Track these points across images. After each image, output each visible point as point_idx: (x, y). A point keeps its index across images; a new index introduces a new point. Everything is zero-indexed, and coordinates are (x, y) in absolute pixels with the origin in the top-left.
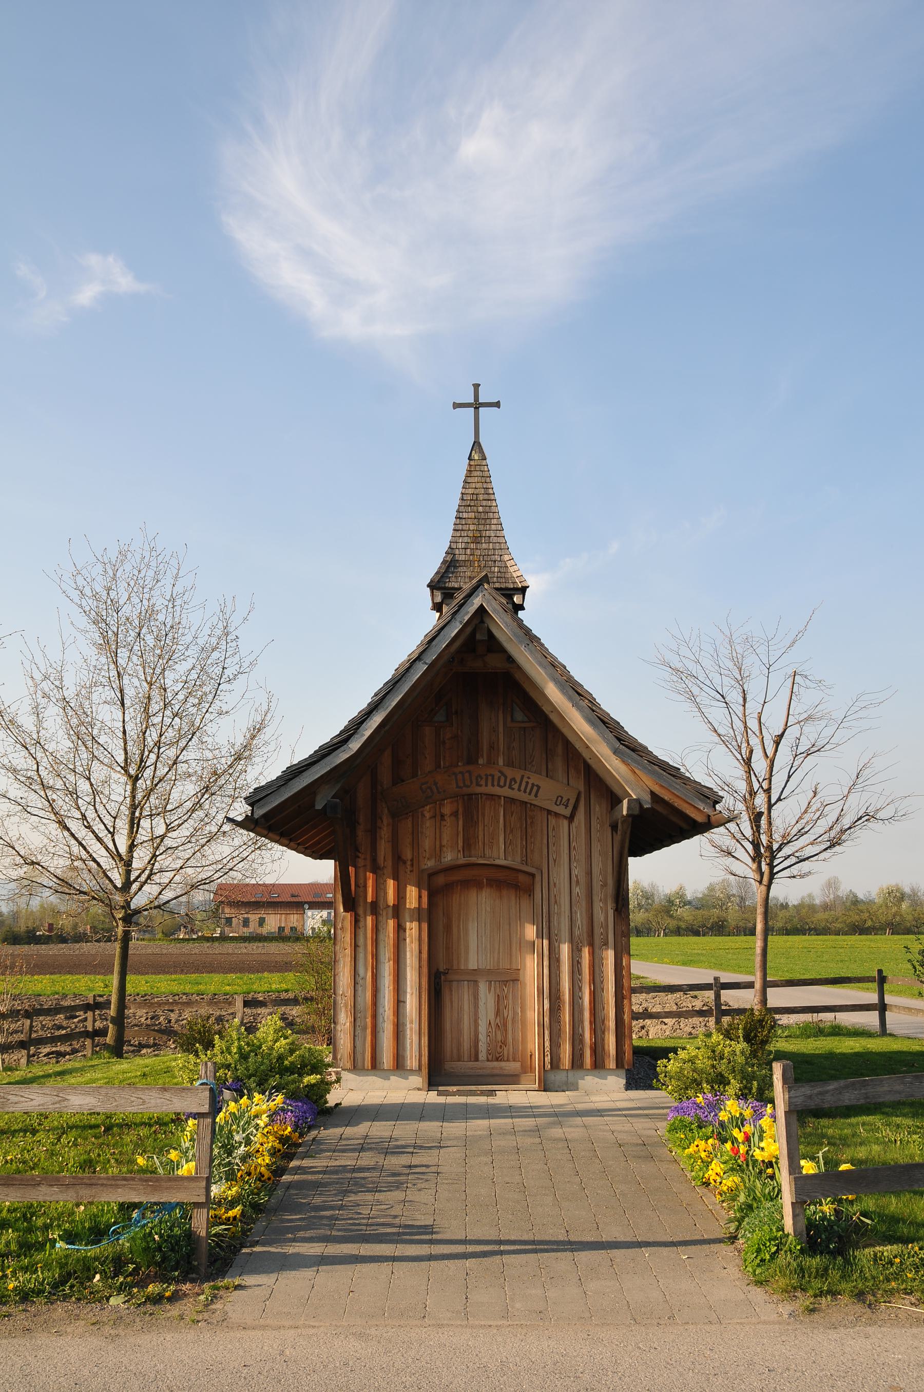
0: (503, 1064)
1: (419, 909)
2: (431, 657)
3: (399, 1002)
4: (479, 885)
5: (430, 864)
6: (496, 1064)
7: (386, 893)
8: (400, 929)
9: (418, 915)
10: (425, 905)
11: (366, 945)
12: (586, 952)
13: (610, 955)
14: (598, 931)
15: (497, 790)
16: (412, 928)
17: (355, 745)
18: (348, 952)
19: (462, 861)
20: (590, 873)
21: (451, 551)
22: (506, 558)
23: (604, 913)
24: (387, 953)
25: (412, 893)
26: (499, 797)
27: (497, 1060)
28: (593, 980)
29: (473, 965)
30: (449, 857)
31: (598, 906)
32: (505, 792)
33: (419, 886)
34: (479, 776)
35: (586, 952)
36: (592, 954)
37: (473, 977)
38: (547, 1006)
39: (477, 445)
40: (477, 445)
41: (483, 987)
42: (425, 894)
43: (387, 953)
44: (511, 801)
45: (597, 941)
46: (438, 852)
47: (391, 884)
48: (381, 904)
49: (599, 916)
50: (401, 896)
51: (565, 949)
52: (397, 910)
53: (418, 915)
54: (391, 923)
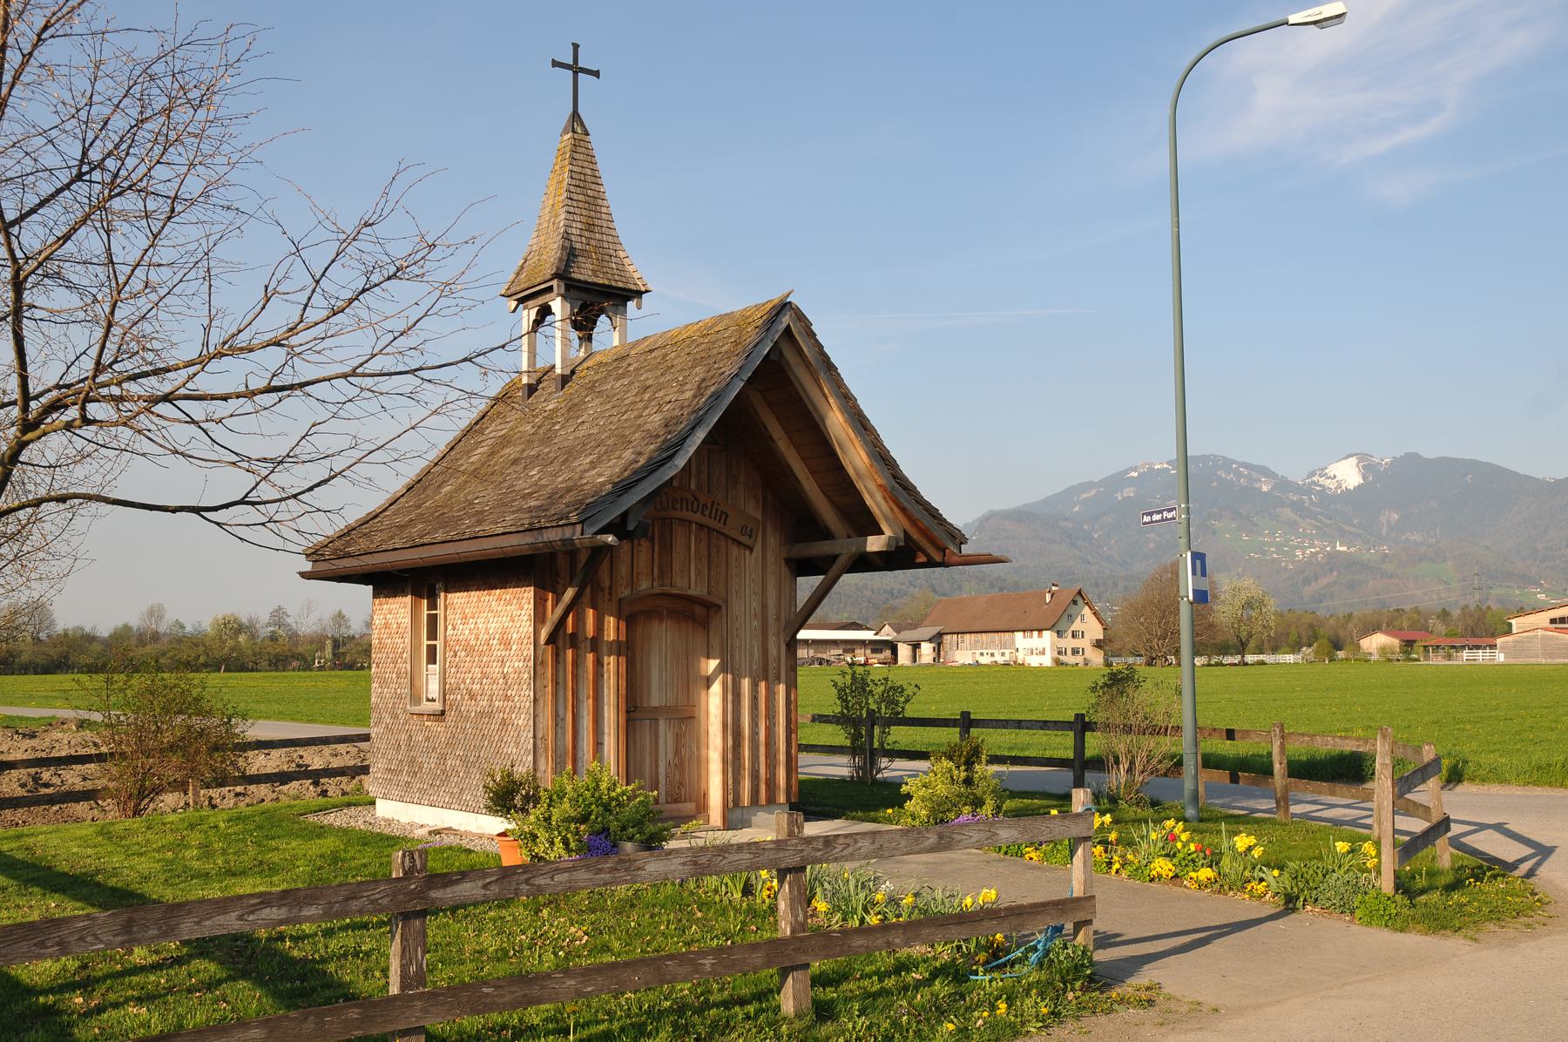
1: (618, 642)
3: (598, 745)
5: (625, 592)
7: (584, 624)
8: (599, 663)
10: (623, 638)
11: (565, 681)
12: (763, 685)
13: (782, 688)
14: (772, 664)
15: (690, 516)
16: (610, 662)
17: (681, 461)
18: (549, 689)
19: (657, 590)
20: (764, 606)
21: (566, 236)
22: (622, 254)
23: (775, 647)
24: (587, 690)
25: (611, 622)
26: (690, 522)
27: (676, 801)
28: (767, 717)
29: (655, 702)
30: (644, 585)
31: (772, 640)
32: (698, 517)
33: (619, 618)
35: (763, 685)
36: (767, 689)
37: (654, 714)
38: (730, 743)
39: (575, 116)
40: (575, 116)
41: (662, 724)
42: (623, 625)
43: (587, 690)
44: (701, 526)
46: (632, 582)
47: (590, 613)
48: (581, 637)
49: (773, 651)
50: (599, 627)
51: (746, 683)
52: (596, 644)
53: (619, 648)
54: (590, 657)
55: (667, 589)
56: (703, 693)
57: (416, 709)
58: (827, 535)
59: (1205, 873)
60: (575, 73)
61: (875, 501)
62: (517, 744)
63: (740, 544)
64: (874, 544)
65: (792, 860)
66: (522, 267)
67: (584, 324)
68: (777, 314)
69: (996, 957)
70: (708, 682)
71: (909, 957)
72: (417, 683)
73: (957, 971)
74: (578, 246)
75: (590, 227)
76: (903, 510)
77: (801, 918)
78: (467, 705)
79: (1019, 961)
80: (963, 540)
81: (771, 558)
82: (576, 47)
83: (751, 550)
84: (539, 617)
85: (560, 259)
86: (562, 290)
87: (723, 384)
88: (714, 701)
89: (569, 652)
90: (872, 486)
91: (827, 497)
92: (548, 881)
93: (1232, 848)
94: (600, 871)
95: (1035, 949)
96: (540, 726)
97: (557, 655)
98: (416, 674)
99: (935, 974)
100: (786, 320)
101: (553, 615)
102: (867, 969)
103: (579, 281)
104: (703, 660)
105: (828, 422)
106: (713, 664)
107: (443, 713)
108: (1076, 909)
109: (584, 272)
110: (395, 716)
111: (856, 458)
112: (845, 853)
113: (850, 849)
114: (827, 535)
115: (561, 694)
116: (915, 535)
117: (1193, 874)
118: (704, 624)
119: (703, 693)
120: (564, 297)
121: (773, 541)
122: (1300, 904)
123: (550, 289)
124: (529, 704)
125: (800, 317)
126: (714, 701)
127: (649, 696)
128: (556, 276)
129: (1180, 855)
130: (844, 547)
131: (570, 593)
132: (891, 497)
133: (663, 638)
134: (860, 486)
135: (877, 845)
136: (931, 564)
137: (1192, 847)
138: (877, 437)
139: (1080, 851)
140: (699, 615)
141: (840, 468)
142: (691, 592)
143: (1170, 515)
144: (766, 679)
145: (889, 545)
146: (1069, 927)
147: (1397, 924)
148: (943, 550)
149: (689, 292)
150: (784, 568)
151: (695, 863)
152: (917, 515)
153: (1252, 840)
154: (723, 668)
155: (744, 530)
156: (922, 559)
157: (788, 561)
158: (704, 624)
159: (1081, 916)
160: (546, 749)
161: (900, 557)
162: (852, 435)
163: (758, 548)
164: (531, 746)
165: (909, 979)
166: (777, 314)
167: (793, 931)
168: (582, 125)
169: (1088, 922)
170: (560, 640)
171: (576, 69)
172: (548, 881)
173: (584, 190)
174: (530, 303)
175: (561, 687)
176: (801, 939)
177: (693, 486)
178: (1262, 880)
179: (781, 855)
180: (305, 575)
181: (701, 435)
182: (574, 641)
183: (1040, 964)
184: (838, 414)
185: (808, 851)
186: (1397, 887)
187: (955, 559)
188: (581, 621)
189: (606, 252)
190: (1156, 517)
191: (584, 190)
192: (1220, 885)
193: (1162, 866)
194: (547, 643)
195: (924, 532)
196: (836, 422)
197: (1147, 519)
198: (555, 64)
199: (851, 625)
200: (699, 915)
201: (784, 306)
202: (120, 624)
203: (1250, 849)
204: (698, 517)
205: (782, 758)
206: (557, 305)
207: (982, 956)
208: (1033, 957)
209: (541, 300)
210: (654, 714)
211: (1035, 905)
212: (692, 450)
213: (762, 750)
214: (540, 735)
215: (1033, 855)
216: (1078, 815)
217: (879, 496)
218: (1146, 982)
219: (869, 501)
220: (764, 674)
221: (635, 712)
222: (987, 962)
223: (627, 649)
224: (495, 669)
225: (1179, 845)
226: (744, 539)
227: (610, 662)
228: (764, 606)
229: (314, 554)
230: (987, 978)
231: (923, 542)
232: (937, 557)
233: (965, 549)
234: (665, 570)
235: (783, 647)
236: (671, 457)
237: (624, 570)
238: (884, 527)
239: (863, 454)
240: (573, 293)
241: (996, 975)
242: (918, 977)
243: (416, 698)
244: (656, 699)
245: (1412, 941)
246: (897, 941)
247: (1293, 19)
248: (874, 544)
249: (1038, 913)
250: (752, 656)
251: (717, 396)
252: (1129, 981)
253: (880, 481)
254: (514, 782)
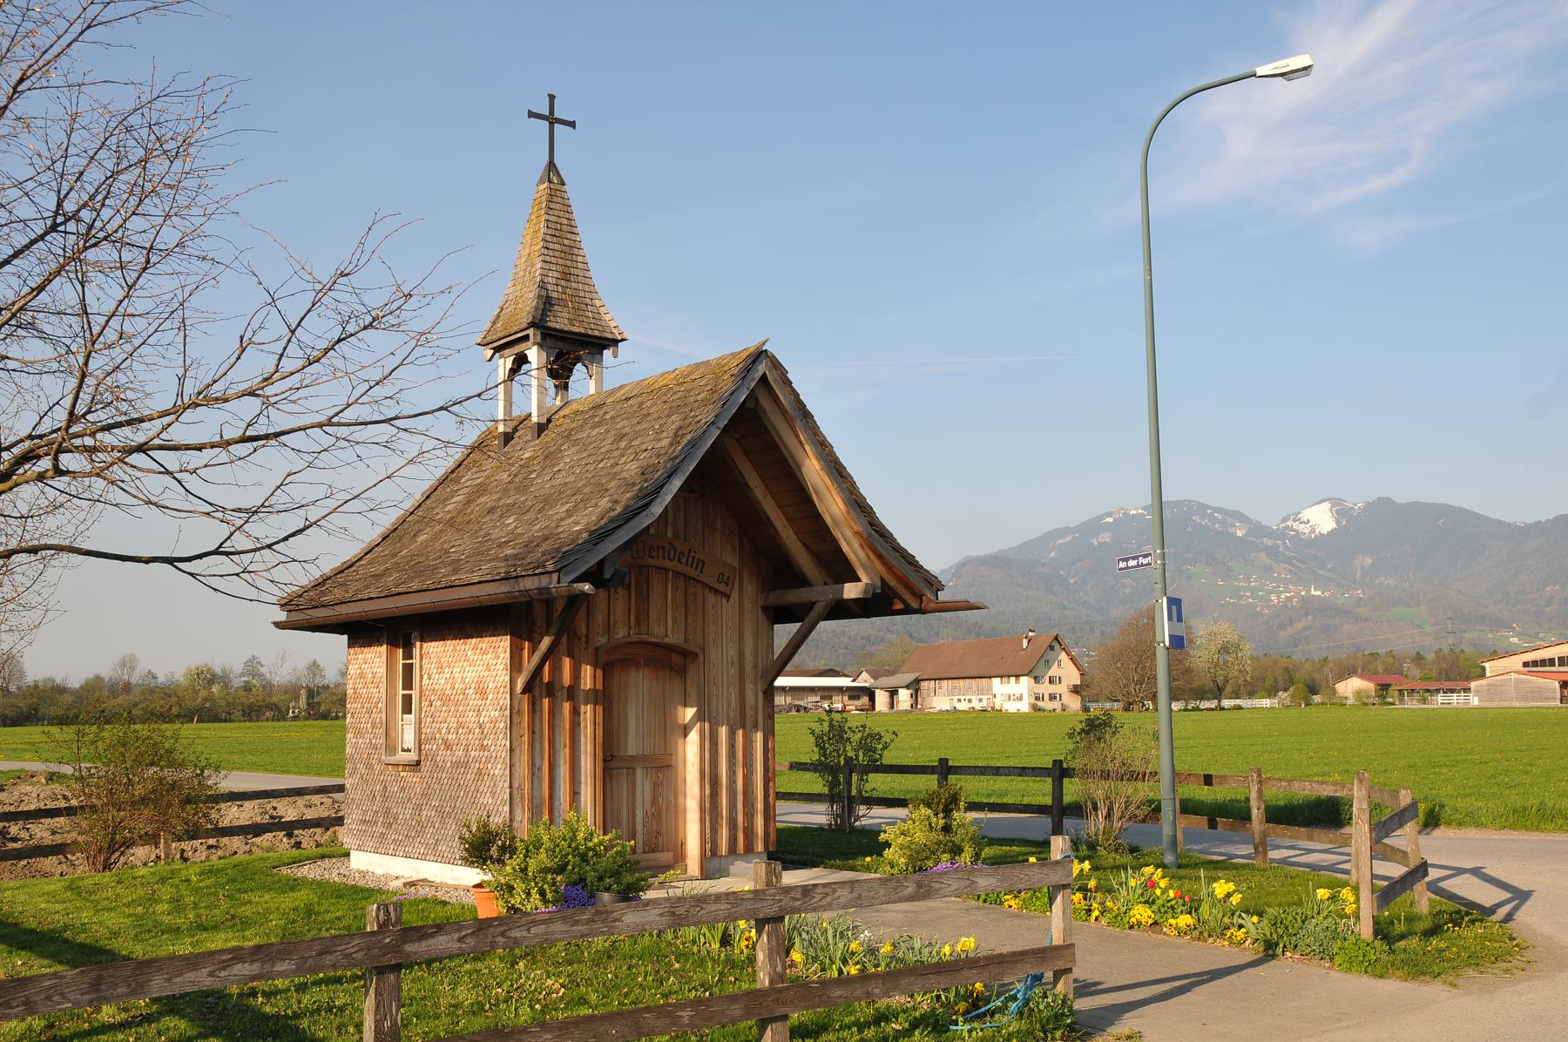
0: (657, 855)
2: (723, 423)
3: (575, 794)
4: (638, 666)
5: (602, 640)
6: (651, 855)
8: (575, 712)
9: (597, 697)
10: (600, 687)
12: (740, 733)
13: (759, 736)
14: (749, 713)
15: (667, 564)
16: (587, 710)
17: (657, 509)
18: (526, 738)
19: (634, 638)
20: (741, 654)
21: (543, 285)
22: (598, 303)
23: (753, 695)
24: (564, 738)
25: (587, 670)
26: (667, 570)
27: (653, 851)
28: (745, 765)
29: (632, 751)
30: (621, 633)
31: (749, 688)
32: (674, 565)
33: (595, 666)
34: (651, 547)
35: (740, 733)
36: (745, 736)
37: (631, 763)
38: (708, 792)
39: (551, 166)
40: (551, 166)
41: (639, 772)
42: (599, 673)
43: (564, 738)
44: (677, 574)
45: (749, 724)
46: (609, 630)
47: (567, 661)
48: (557, 684)
49: (750, 699)
50: (576, 676)
52: (572, 692)
53: (597, 697)
54: (567, 706)
55: (644, 637)
56: (680, 741)
57: (391, 760)
58: (804, 582)
59: (1185, 920)
60: (551, 124)
61: (852, 547)
62: (493, 794)
63: (716, 591)
64: (851, 591)
65: (769, 910)
66: (498, 316)
67: (560, 372)
68: (753, 362)
69: (976, 1007)
70: (686, 730)
71: (889, 1007)
72: (392, 733)
73: (937, 1021)
74: (554, 295)
75: (566, 276)
76: (880, 557)
77: (779, 969)
78: (445, 757)
79: (1002, 1010)
80: (940, 587)
81: (748, 605)
82: (552, 97)
83: (728, 597)
84: (515, 665)
85: (536, 308)
86: (539, 339)
87: (700, 432)
88: (691, 749)
89: (546, 701)
90: (849, 534)
91: (805, 545)
92: (525, 933)
93: (1211, 895)
94: (577, 922)
95: (1014, 998)
96: (516, 775)
97: (534, 704)
98: (391, 724)
99: (915, 1025)
100: (762, 368)
101: (529, 664)
102: (847, 1020)
103: (555, 329)
104: (680, 708)
105: (804, 470)
106: (690, 712)
107: (418, 763)
108: (1056, 957)
109: (560, 321)
110: (370, 767)
111: (832, 506)
112: (824, 902)
113: (829, 899)
114: (804, 582)
115: (537, 743)
116: (892, 582)
117: (1173, 921)
118: (682, 672)
119: (680, 741)
120: (540, 345)
121: (750, 588)
122: (1279, 951)
123: (526, 338)
124: (505, 754)
125: (776, 365)
126: (691, 749)
127: (626, 744)
128: (532, 325)
129: (1159, 902)
130: (820, 594)
131: (546, 642)
132: (868, 544)
133: (639, 686)
134: (836, 533)
135: (855, 895)
136: (908, 610)
137: (1171, 894)
138: (853, 484)
139: (1059, 899)
140: (676, 663)
141: (817, 516)
142: (669, 640)
143: (1145, 561)
144: (744, 727)
145: (865, 592)
146: (1049, 976)
147: (1377, 970)
148: (920, 597)
149: (666, 341)
150: (761, 615)
151: (673, 914)
152: (893, 562)
153: (1231, 887)
154: (700, 717)
155: (721, 578)
156: (899, 606)
157: (765, 609)
158: (682, 672)
159: (1060, 965)
160: (522, 798)
161: (877, 604)
162: (829, 483)
163: (735, 596)
164: (507, 797)
165: (888, 1030)
166: (753, 362)
167: (771, 982)
168: (559, 175)
169: (1068, 971)
170: (536, 689)
171: (552, 120)
172: (525, 933)
173: (560, 239)
174: (507, 352)
175: (537, 736)
176: (780, 990)
177: (669, 534)
178: (1241, 927)
179: (759, 905)
180: (280, 625)
181: (677, 483)
182: (551, 690)
183: (1020, 1014)
184: (814, 461)
185: (786, 901)
186: (1376, 933)
187: (932, 605)
188: (556, 670)
189: (583, 301)
190: (1132, 563)
191: (560, 239)
192: (1200, 931)
193: (1142, 913)
194: (523, 692)
195: (902, 580)
196: (812, 470)
197: (1122, 565)
198: (532, 115)
200: (677, 966)
201: (760, 355)
202: (91, 676)
203: (1229, 895)
204: (674, 565)
205: (760, 806)
206: (533, 354)
207: (962, 1006)
208: (1013, 1006)
209: (517, 349)
210: (631, 763)
211: (1014, 954)
212: (669, 498)
213: (740, 798)
214: (516, 785)
215: (1012, 902)
216: (1057, 862)
217: (855, 543)
218: (1127, 1031)
219: (845, 548)
220: (741, 722)
221: (611, 762)
222: (967, 1012)
223: (604, 698)
224: (471, 718)
225: (1158, 892)
226: (722, 587)
227: (587, 710)
228: (741, 654)
229: (286, 605)
230: (967, 1027)
231: (900, 590)
232: (915, 605)
233: (942, 596)
234: (642, 619)
235: (761, 695)
236: (647, 505)
237: (600, 618)
238: (861, 574)
239: (839, 501)
240: (549, 342)
241: (975, 1025)
242: (898, 1027)
243: (391, 749)
244: (633, 747)
245: (1391, 987)
246: (877, 991)
247: (1260, 71)
248: (851, 591)
249: (1017, 962)
250: (729, 703)
251: (694, 444)
252: (1109, 1030)
253: (856, 528)
254: (490, 833)
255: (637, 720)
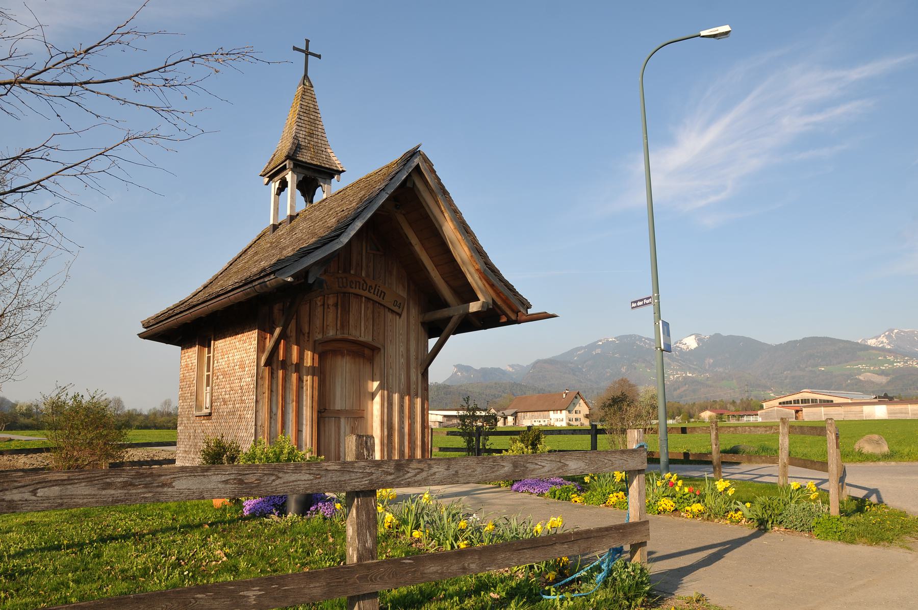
1: (313, 367)
2: (390, 191)
3: (299, 431)
4: (343, 355)
5: (319, 337)
7: (291, 355)
8: (300, 380)
10: (316, 365)
11: (277, 391)
12: (407, 398)
14: (413, 386)
15: (361, 292)
16: (308, 380)
17: (344, 240)
19: (339, 336)
20: (408, 350)
21: (296, 138)
22: (329, 151)
23: (415, 375)
24: (292, 396)
25: (308, 355)
26: (361, 296)
28: (410, 418)
29: (338, 406)
30: (331, 333)
32: (366, 293)
33: (314, 352)
35: (407, 398)
36: (410, 400)
37: (338, 414)
38: (386, 433)
39: (306, 76)
40: (306, 76)
41: (342, 420)
42: (316, 356)
43: (292, 396)
45: (412, 393)
46: (323, 330)
47: (295, 348)
49: (413, 378)
51: (396, 397)
52: (298, 367)
53: (313, 371)
54: (294, 376)
55: (346, 336)
56: (370, 402)
57: (198, 414)
58: (446, 305)
59: (697, 507)
60: (307, 55)
61: (474, 279)
62: (246, 429)
63: (393, 311)
64: (474, 307)
65: (361, 483)
66: (272, 159)
67: (307, 188)
68: (411, 156)
69: (564, 577)
70: (373, 396)
71: (489, 576)
72: (200, 398)
73: (531, 590)
74: (303, 144)
75: (311, 135)
76: (492, 286)
77: (369, 544)
78: (225, 409)
79: (586, 579)
80: (529, 306)
81: (412, 321)
82: (307, 41)
83: (400, 315)
84: (260, 348)
85: (291, 149)
86: (292, 166)
87: (374, 194)
88: (376, 407)
89: (280, 372)
90: (472, 270)
91: (446, 282)
92: (27, 496)
93: (714, 489)
94: (108, 486)
95: (599, 569)
96: (260, 418)
97: (272, 373)
98: (200, 392)
99: (512, 594)
100: (417, 160)
101: (269, 344)
102: (451, 589)
103: (302, 161)
104: (370, 382)
105: (444, 228)
106: (376, 384)
107: (210, 414)
108: (631, 535)
109: (305, 157)
110: (189, 419)
111: (462, 252)
112: (419, 477)
113: (424, 474)
114: (446, 305)
115: (274, 398)
116: (499, 302)
117: (688, 508)
118: (371, 360)
119: (370, 402)
120: (293, 171)
121: (414, 312)
122: (769, 526)
123: (284, 168)
124: (253, 404)
125: (426, 160)
126: (376, 407)
127: (334, 403)
128: (288, 157)
129: (679, 495)
130: (455, 311)
131: (278, 331)
132: (483, 276)
133: (344, 368)
134: (464, 269)
135: (452, 471)
136: (510, 322)
137: (686, 490)
138: (475, 237)
139: (635, 483)
140: (367, 353)
141: (453, 260)
142: (362, 339)
143: (648, 302)
144: (409, 395)
145: (483, 306)
146: (627, 548)
147: (849, 538)
148: (517, 312)
149: (361, 160)
150: (421, 329)
151: (241, 482)
152: (502, 290)
153: (727, 484)
154: (381, 387)
155: (395, 303)
156: (504, 319)
157: (423, 324)
158: (371, 360)
159: (637, 539)
160: (263, 432)
161: (490, 319)
162: (459, 237)
163: (404, 315)
164: (253, 431)
165: (487, 598)
166: (411, 156)
167: (360, 558)
168: (309, 82)
169: (643, 544)
170: (272, 362)
171: (307, 53)
172: (27, 496)
173: (308, 114)
174: (276, 179)
175: (274, 394)
176: (368, 567)
177: (363, 275)
178: (737, 510)
179: (346, 477)
180: (142, 336)
181: (358, 225)
182: (284, 365)
183: (605, 583)
184: (450, 223)
185: (377, 474)
186: (841, 512)
187: (524, 317)
188: (288, 351)
189: (320, 148)
190: (640, 303)
191: (308, 114)
192: (708, 515)
193: (667, 504)
194: (265, 365)
195: (506, 301)
196: (449, 229)
197: (634, 305)
198: (295, 49)
199: (462, 356)
200: (331, 540)
201: (414, 153)
203: (726, 489)
204: (366, 293)
205: (419, 443)
206: (289, 176)
207: (551, 576)
208: (600, 577)
209: (281, 176)
210: (338, 414)
211: (600, 530)
212: (353, 233)
213: (406, 437)
214: (259, 424)
215: (577, 499)
216: (634, 451)
217: (476, 276)
218: (694, 595)
219: (470, 279)
220: (408, 391)
221: (323, 413)
222: (556, 580)
223: (320, 372)
224: (236, 385)
225: (677, 489)
226: (396, 309)
227: (308, 380)
228: (408, 350)
229: (146, 325)
230: (558, 597)
231: (504, 307)
232: (513, 317)
233: (530, 311)
234: (344, 325)
235: (420, 376)
236: (338, 236)
237: (318, 322)
238: (480, 296)
239: (466, 249)
240: (299, 169)
241: (567, 595)
242: (495, 596)
243: (199, 407)
244: (339, 404)
245: (862, 551)
246: (473, 566)
247: (703, 33)
248: (474, 307)
249: (603, 537)
250: (400, 380)
251: (371, 201)
252: (678, 593)
253: (477, 267)
254: (223, 447)
255: (342, 388)
